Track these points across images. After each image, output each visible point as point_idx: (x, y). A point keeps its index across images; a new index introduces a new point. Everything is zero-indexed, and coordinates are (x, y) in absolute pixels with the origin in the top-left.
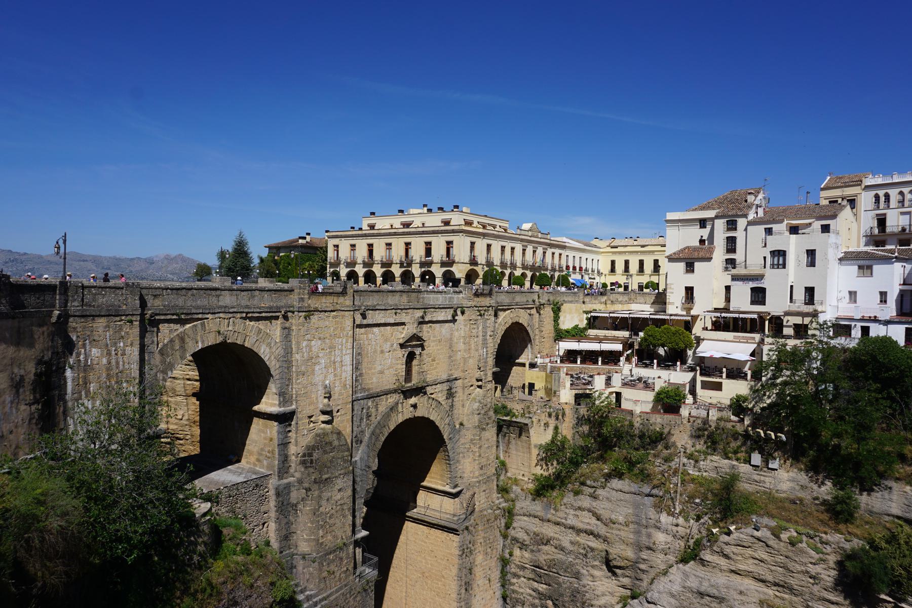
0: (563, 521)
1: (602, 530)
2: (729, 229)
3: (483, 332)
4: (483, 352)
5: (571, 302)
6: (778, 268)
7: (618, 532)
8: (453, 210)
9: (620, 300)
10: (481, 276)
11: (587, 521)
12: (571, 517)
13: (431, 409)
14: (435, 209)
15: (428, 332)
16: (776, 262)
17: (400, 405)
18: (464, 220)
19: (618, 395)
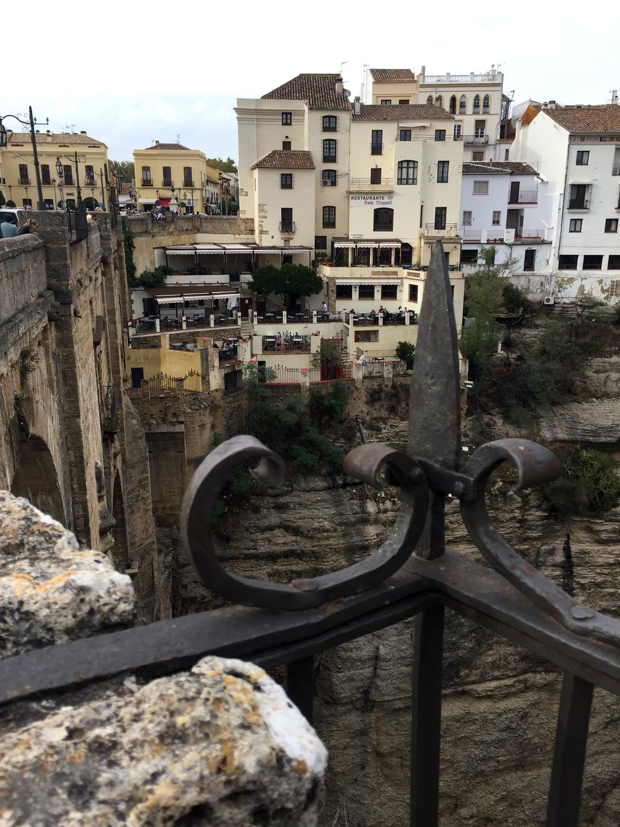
0: (252, 551)
1: (307, 545)
2: (325, 129)
6: (407, 184)
7: (326, 542)
11: (283, 542)
12: (261, 543)
16: (404, 176)
19: (262, 363)
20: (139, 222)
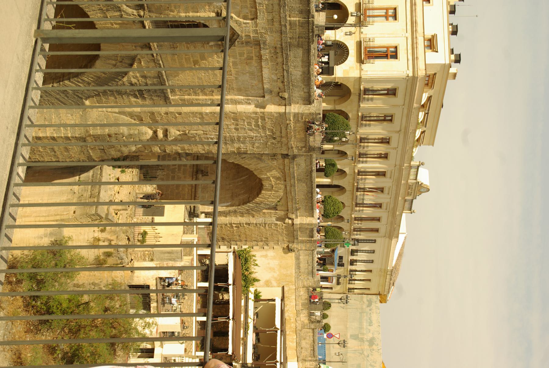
3: (245, 138)
4: (212, 139)
5: (298, 267)
8: (452, 51)
9: (304, 343)
10: (338, 107)
13: (114, 62)
14: (454, 19)
15: (241, 55)
17: (118, 13)
18: (435, 74)
20: (310, 268)
